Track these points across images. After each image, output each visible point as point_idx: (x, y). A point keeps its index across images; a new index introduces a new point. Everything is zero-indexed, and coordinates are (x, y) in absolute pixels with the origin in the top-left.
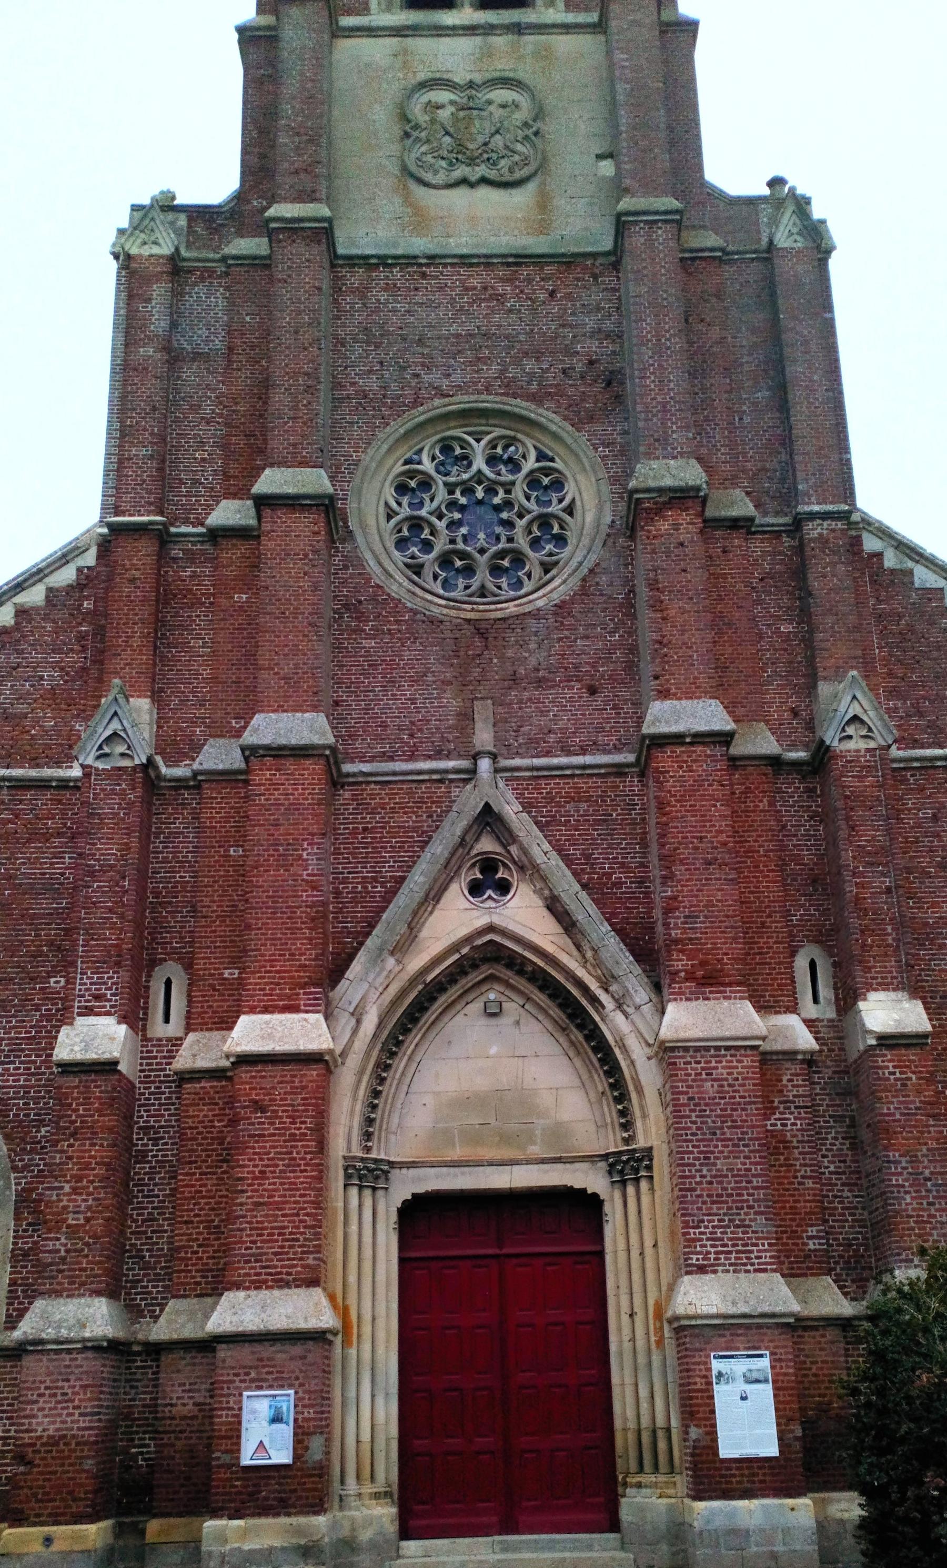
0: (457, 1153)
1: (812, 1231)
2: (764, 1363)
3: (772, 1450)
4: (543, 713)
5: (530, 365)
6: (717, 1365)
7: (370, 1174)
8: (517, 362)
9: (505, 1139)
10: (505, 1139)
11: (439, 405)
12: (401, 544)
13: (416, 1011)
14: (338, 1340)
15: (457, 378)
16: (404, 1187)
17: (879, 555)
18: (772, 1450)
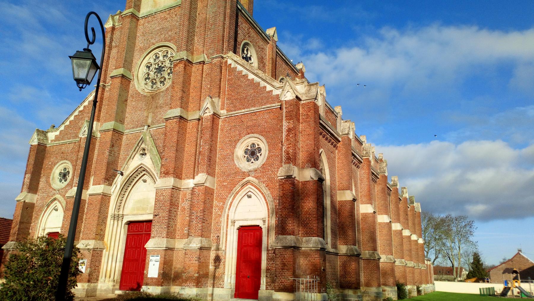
0: (135, 212)
1: (186, 229)
2: (159, 258)
3: (156, 276)
4: (160, 114)
5: (170, 33)
6: (151, 258)
7: (117, 217)
8: (168, 33)
9: (143, 209)
10: (143, 209)
11: (153, 47)
12: (146, 79)
13: (129, 183)
14: (104, 251)
15: (157, 40)
16: (125, 220)
17: (231, 64)
18: (156, 276)
